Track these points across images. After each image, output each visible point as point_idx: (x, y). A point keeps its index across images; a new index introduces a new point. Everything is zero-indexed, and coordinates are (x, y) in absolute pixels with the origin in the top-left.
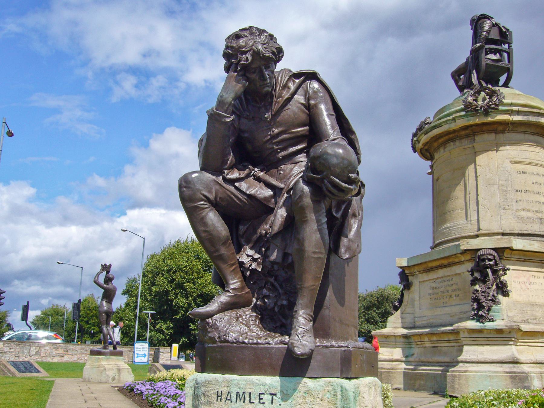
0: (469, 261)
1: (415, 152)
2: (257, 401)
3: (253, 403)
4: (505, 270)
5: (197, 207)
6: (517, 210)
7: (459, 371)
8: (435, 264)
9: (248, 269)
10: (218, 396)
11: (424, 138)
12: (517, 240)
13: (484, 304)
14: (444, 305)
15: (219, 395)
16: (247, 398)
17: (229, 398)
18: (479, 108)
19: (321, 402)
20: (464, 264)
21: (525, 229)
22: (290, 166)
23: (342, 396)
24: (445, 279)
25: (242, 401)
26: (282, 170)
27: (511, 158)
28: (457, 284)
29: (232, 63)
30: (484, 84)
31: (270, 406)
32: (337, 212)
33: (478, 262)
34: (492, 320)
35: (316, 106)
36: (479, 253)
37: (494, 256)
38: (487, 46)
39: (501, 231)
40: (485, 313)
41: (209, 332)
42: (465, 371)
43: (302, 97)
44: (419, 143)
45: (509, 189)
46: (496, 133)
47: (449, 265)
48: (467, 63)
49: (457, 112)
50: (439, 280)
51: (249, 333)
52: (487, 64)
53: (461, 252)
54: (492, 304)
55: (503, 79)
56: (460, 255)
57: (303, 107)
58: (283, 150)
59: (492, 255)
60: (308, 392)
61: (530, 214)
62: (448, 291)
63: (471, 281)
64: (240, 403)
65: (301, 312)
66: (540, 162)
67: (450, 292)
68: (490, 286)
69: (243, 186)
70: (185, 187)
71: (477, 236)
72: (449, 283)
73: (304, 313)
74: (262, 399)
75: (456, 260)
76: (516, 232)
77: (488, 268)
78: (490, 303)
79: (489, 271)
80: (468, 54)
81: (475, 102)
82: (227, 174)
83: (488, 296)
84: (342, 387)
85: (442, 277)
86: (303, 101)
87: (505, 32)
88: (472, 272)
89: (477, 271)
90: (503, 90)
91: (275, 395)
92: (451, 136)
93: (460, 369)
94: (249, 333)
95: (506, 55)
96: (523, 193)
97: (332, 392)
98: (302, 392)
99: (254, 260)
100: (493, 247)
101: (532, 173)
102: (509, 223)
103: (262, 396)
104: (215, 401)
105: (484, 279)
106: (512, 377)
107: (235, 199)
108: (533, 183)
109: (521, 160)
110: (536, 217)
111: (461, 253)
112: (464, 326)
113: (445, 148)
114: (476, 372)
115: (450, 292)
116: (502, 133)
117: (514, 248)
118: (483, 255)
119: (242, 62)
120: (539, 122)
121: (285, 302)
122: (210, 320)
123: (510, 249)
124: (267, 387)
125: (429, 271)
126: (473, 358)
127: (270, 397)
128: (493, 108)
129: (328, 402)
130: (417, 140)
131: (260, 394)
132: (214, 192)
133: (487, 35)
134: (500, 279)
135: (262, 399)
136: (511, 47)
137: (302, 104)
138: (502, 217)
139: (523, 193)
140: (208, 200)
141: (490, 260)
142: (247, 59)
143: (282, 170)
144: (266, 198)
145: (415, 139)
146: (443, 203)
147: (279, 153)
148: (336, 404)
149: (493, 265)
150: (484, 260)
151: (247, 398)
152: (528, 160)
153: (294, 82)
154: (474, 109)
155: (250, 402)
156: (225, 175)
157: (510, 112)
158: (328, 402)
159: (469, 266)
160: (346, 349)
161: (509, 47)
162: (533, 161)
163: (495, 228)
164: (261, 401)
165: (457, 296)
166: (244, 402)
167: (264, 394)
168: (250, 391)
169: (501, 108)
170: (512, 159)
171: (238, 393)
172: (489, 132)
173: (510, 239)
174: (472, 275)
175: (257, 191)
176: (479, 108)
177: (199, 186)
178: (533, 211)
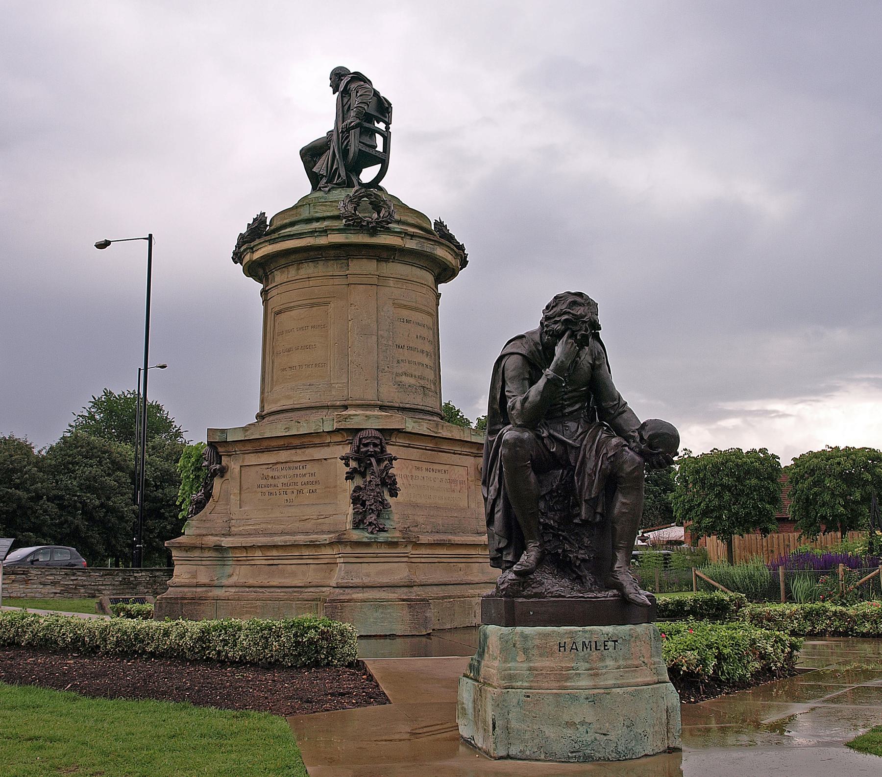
4: (392, 459)
6: (397, 375)
8: (274, 443)
16: (594, 646)
24: (291, 465)
27: (394, 300)
33: (359, 447)
37: (381, 440)
42: (349, 601)
45: (390, 343)
46: (377, 260)
47: (303, 447)
58: (569, 405)
61: (412, 381)
62: (295, 484)
72: (298, 472)
75: (317, 441)
76: (397, 405)
77: (371, 456)
79: (373, 460)
89: (355, 460)
92: (312, 253)
95: (379, 140)
104: (557, 651)
106: (410, 606)
113: (298, 269)
116: (386, 262)
128: (383, 227)
134: (387, 473)
150: (366, 445)
172: (369, 258)
174: (347, 465)
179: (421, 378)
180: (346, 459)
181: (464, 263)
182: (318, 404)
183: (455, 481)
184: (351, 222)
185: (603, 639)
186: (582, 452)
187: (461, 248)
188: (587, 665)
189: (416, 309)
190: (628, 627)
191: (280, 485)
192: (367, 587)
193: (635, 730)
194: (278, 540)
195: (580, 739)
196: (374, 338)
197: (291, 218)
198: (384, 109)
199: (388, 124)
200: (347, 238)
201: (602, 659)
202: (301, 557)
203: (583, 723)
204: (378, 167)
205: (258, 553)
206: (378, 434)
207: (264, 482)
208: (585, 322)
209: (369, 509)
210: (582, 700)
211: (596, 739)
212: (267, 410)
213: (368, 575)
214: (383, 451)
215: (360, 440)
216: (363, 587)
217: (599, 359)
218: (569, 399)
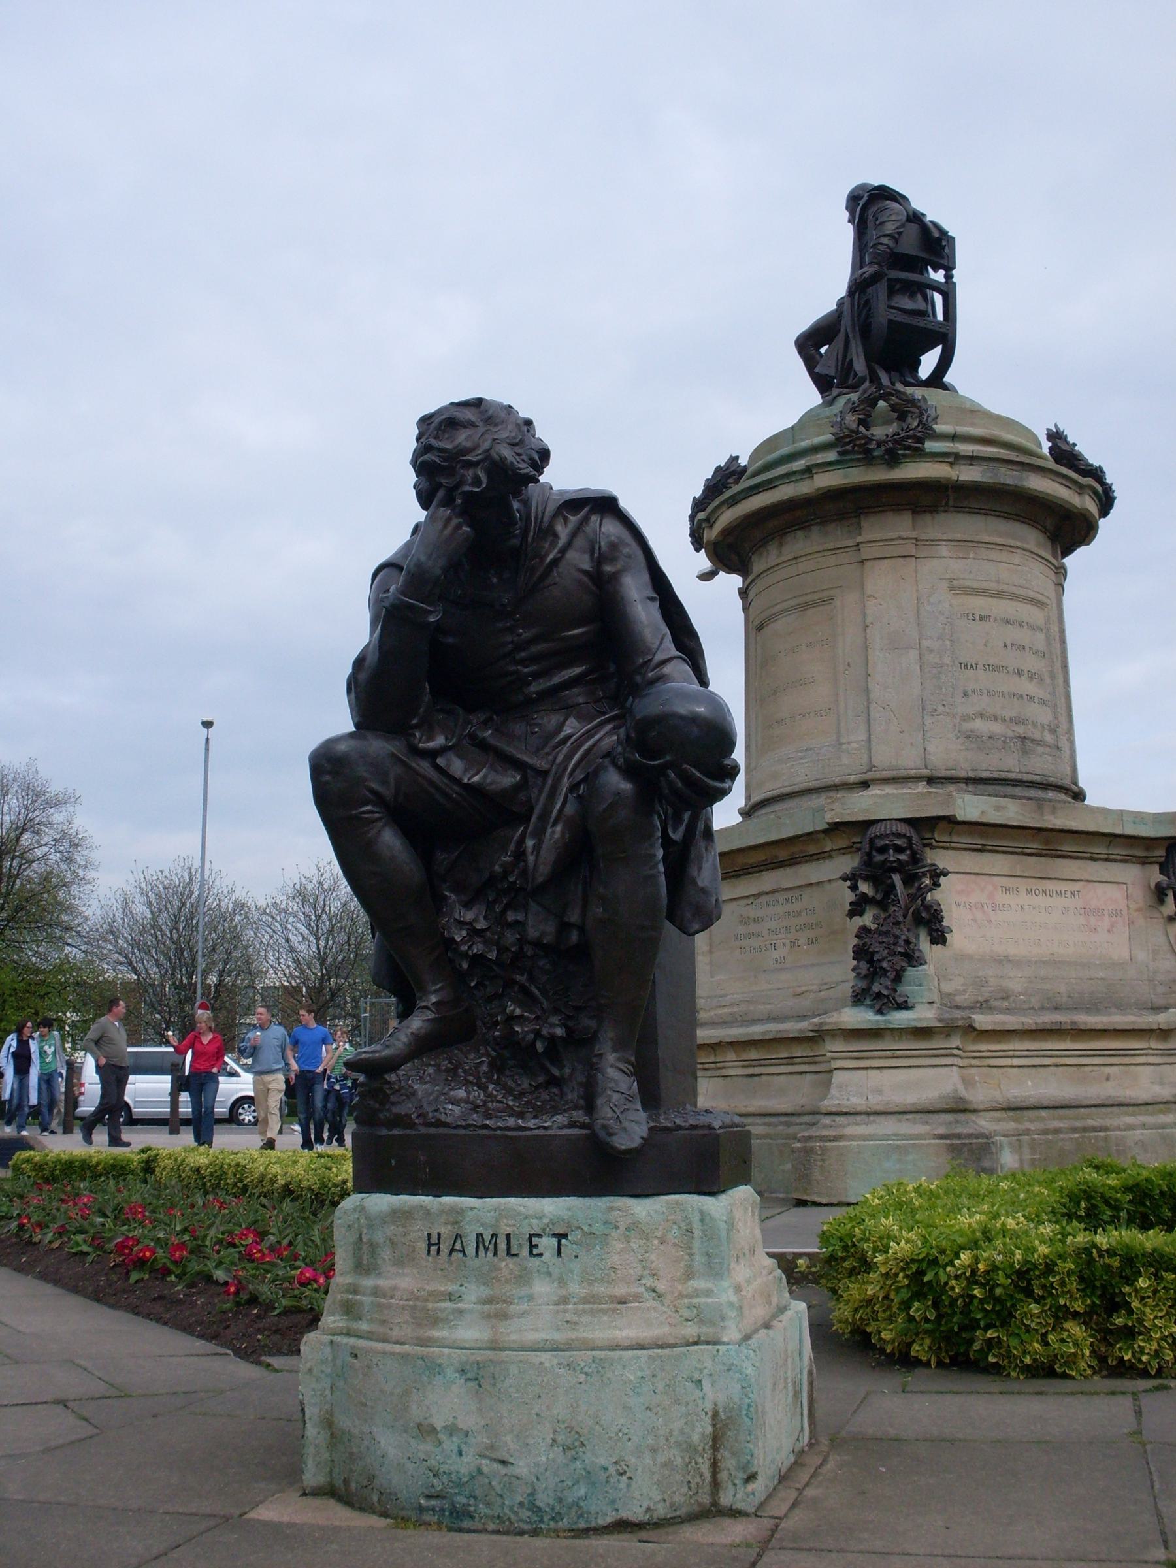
0: (844, 851)
1: (697, 550)
2: (525, 1252)
3: (516, 1255)
4: (937, 875)
5: (357, 818)
6: (966, 718)
7: (822, 1138)
8: (754, 858)
9: (465, 955)
10: (430, 1245)
11: (727, 517)
12: (967, 797)
13: (885, 964)
14: (778, 966)
15: (433, 1244)
16: (503, 1246)
17: (458, 1246)
18: (873, 446)
19: (662, 1247)
20: (830, 857)
21: (984, 766)
22: (554, 719)
23: (703, 1231)
25: (490, 1254)
26: (538, 725)
27: (951, 580)
28: (812, 911)
29: (440, 485)
30: (885, 379)
31: (556, 1260)
32: (675, 830)
33: (869, 855)
34: (904, 1006)
35: (615, 577)
36: (873, 831)
37: (910, 839)
38: (894, 274)
39: (925, 772)
40: (887, 988)
41: (393, 1104)
42: (836, 1139)
43: (587, 557)
44: (711, 527)
45: (947, 660)
46: (914, 512)
47: (793, 862)
48: (837, 315)
49: (816, 449)
50: (763, 899)
51: (490, 1105)
52: (890, 321)
53: (826, 826)
54: (904, 964)
55: (928, 362)
56: (822, 836)
57: (586, 579)
58: (536, 676)
59: (904, 836)
60: (634, 1227)
61: (997, 728)
63: (851, 903)
64: (487, 1258)
65: (611, 1057)
66: (1022, 592)
67: (793, 930)
68: (901, 919)
69: (457, 766)
70: (330, 773)
71: (865, 785)
73: (619, 1059)
74: (536, 1246)
75: (812, 849)
76: (963, 774)
77: (894, 870)
78: (900, 962)
79: (897, 878)
80: (842, 291)
81: (862, 428)
82: (420, 741)
83: (895, 944)
84: (702, 1213)
85: (773, 892)
86: (587, 566)
87: (939, 240)
88: (852, 879)
89: (866, 879)
90: (933, 396)
91: (565, 1236)
93: (825, 1133)
94: (490, 1105)
95: (938, 299)
96: (981, 672)
97: (683, 1225)
98: (622, 1228)
99: (475, 933)
100: (909, 816)
101: (1002, 620)
102: (946, 752)
103: (535, 1240)
104: (424, 1255)
105: (884, 900)
106: (952, 1149)
107: (438, 797)
108: (1005, 646)
109: (976, 585)
110: (1010, 734)
111: (824, 831)
112: (835, 1023)
114: (865, 1138)
115: (793, 930)
116: (931, 512)
117: (959, 819)
118: (882, 836)
119: (467, 488)
120: (1023, 488)
121: (559, 1032)
122: (392, 1077)
123: (950, 821)
124: (546, 1221)
125: (739, 876)
126: (856, 1102)
127: (554, 1241)
128: (909, 448)
129: (675, 1244)
130: (707, 520)
131: (531, 1236)
132: (392, 781)
133: (891, 244)
134: (924, 900)
135: (536, 1246)
136: (952, 277)
137: (586, 572)
138: (928, 735)
139: (981, 672)
140: (379, 800)
141: (899, 850)
142: (477, 481)
143: (538, 725)
144: (504, 792)
145: (701, 516)
146: (775, 693)
147: (530, 683)
148: (690, 1248)
149: (907, 863)
150: (883, 850)
151: (503, 1246)
152: (994, 586)
153: (566, 520)
154: (860, 446)
155: (509, 1253)
156: (416, 741)
157: (951, 460)
158: (675, 1244)
159: (847, 863)
160: (706, 1132)
161: (946, 276)
162: (1005, 588)
163: (910, 762)
164: (535, 1251)
165: (810, 942)
166: (495, 1254)
167: (539, 1236)
168: (508, 1230)
169: (931, 446)
170: (955, 583)
171: (479, 1237)
172: (897, 508)
173: (950, 796)
174: (854, 888)
175: (485, 777)
176: (873, 446)
177: (362, 771)
178: (1004, 720)
179: (1018, 721)
180: (852, 879)
181: (1106, 501)
182: (818, 784)
183: (1098, 912)
184: (849, 447)
185: (526, 1231)
186: (550, 781)
187: (1097, 474)
188: (485, 1292)
189: (999, 595)
190: (431, 1198)
191: (765, 933)
192: (877, 1113)
193: (588, 1458)
194: (756, 1031)
195: (444, 1468)
196: (913, 655)
197: (777, 456)
198: (935, 246)
199: (949, 269)
200: (846, 476)
201: (523, 1278)
202: (790, 1061)
203: (452, 1430)
204: (938, 350)
205: (731, 1056)
206: (904, 829)
207: (742, 929)
208: (474, 464)
209: (881, 972)
210: (450, 1373)
211: (480, 1471)
212: (756, 798)
213: (879, 1091)
214: (916, 859)
215: (872, 841)
216: (868, 1114)
217: (613, 560)
218: (533, 659)
